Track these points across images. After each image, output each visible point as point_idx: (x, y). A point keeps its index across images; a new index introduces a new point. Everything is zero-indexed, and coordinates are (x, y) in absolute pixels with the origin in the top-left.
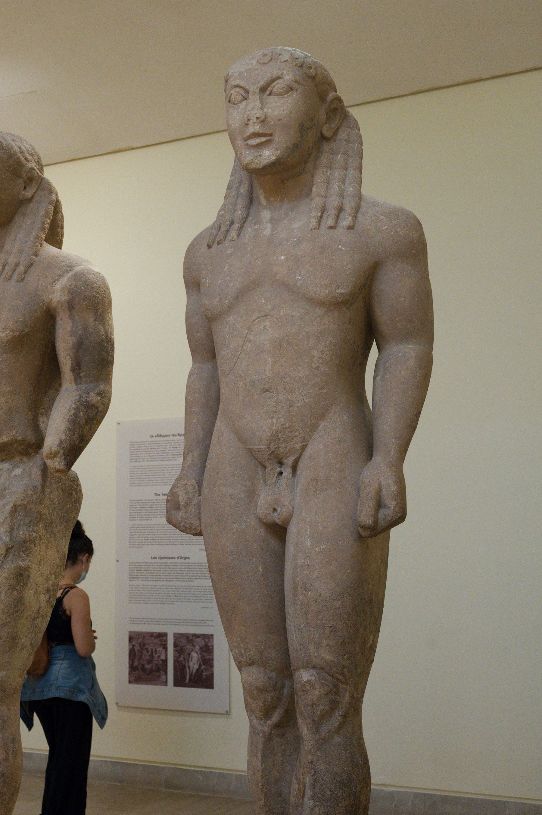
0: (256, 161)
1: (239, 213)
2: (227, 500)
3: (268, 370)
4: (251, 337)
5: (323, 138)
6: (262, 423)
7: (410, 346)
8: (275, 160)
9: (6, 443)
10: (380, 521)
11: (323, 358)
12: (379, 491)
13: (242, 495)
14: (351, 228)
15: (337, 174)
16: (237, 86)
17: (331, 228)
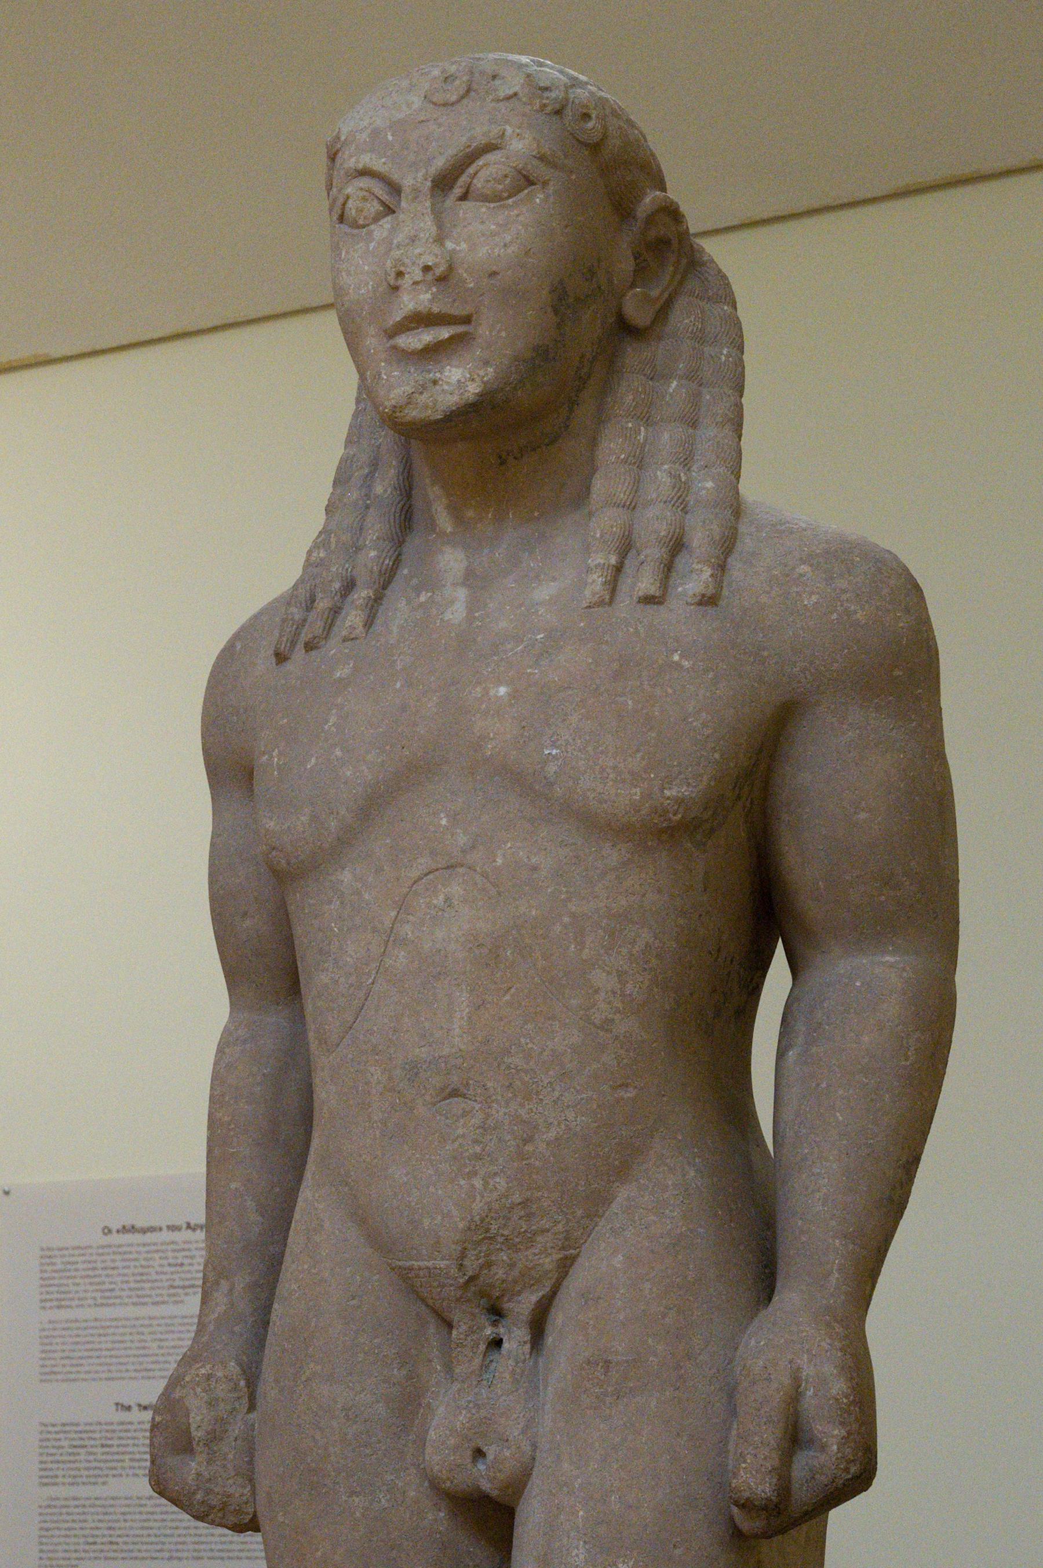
0: (423, 399)
1: (372, 556)
2: (334, 1423)
3: (457, 1031)
4: (407, 930)
5: (626, 329)
6: (438, 1190)
7: (888, 958)
8: (481, 395)
10: (795, 1486)
11: (623, 995)
12: (795, 1397)
13: (380, 1408)
14: (709, 601)
15: (668, 437)
16: (365, 173)
17: (648, 600)
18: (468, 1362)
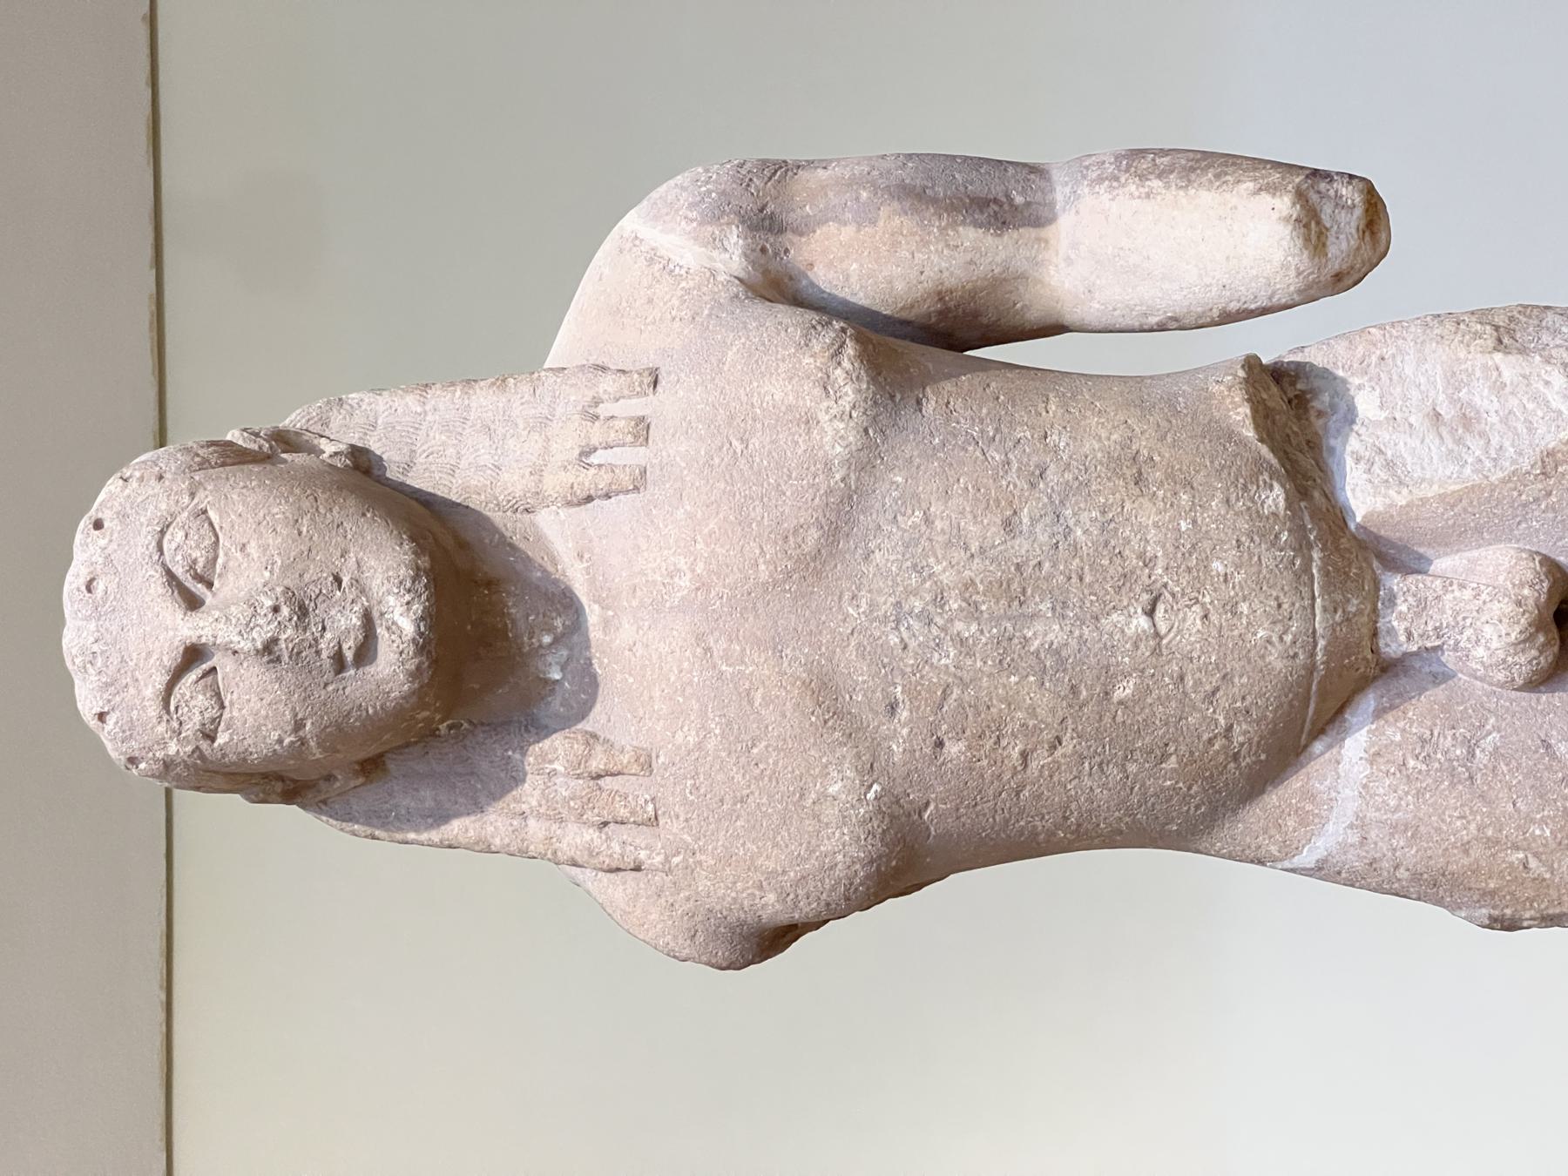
9: (1255, 411)
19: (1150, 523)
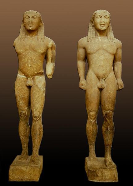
14: (115, 42)
18: (101, 81)
19: (35, 67)
